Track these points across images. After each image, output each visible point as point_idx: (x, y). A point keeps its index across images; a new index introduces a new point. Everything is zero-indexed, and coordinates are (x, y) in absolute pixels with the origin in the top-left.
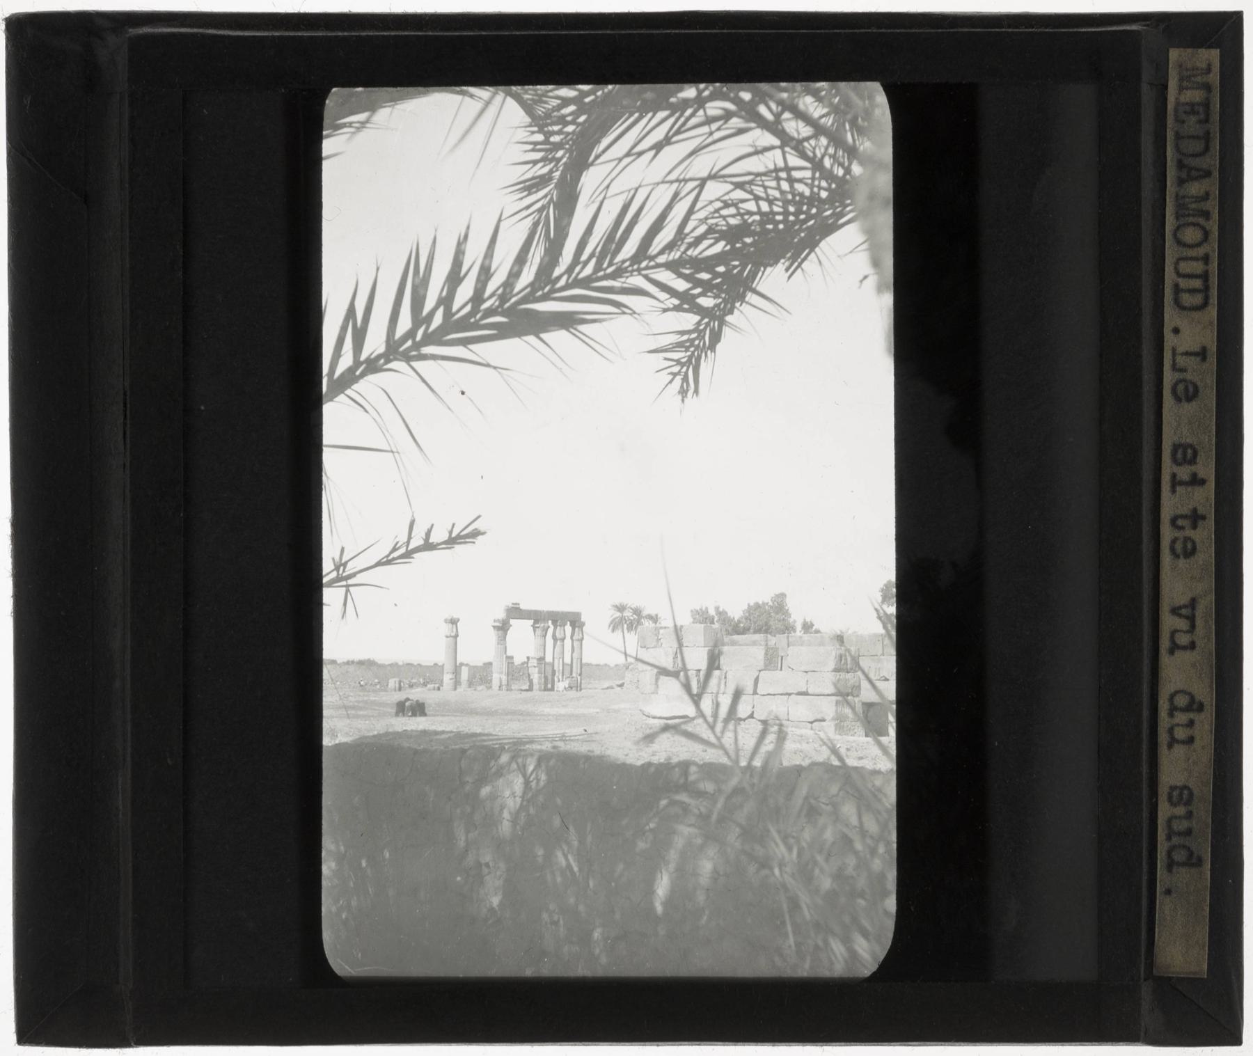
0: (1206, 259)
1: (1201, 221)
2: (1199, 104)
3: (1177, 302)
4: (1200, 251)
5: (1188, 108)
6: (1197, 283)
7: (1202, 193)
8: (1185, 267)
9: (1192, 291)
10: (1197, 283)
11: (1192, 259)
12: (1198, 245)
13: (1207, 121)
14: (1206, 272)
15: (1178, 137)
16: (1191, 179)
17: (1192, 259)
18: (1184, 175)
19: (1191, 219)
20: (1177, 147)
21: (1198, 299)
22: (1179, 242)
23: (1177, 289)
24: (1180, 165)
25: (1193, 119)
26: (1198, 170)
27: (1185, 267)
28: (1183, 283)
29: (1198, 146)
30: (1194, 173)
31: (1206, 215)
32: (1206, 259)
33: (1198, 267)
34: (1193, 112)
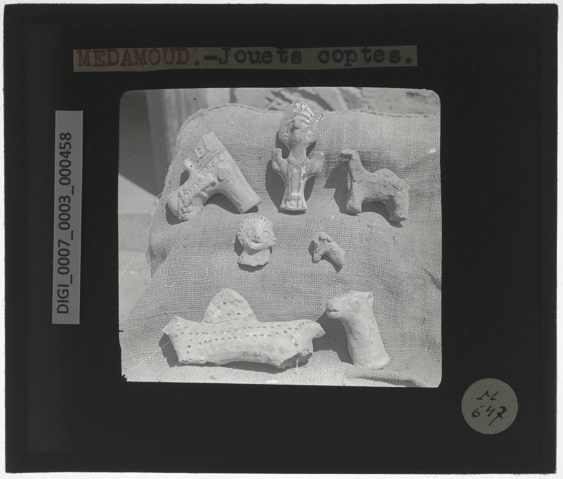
6: (176, 53)
8: (169, 59)
15: (110, 64)
26: (125, 56)
28: (176, 60)
29: (113, 55)
31: (143, 51)
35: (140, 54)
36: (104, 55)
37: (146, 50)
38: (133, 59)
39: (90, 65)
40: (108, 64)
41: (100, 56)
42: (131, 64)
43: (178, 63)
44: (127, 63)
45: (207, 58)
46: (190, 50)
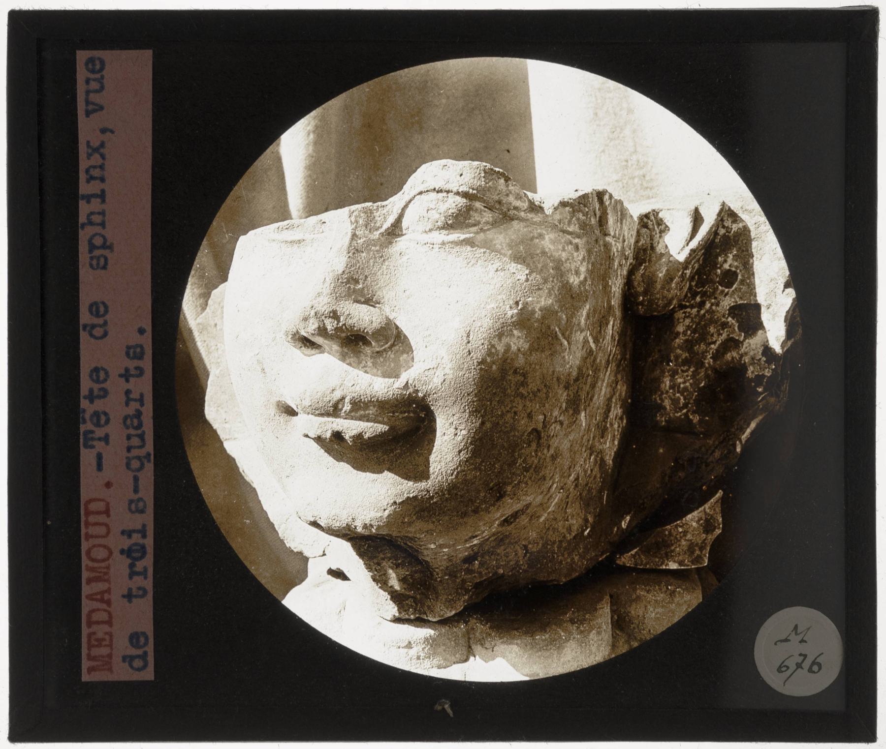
0: (88, 537)
1: (91, 564)
2: (94, 646)
3: (108, 504)
4: (92, 542)
5: (104, 643)
6: (92, 519)
7: (93, 584)
8: (102, 530)
9: (98, 513)
11: (97, 537)
12: (94, 546)
13: (90, 636)
14: (87, 527)
15: (109, 623)
17: (97, 537)
19: (96, 565)
20: (110, 614)
21: (93, 507)
22: (105, 547)
23: (107, 512)
24: (108, 602)
25: (100, 635)
26: (96, 600)
28: (102, 518)
30: (99, 597)
31: (90, 569)
33: (92, 530)
34: (100, 641)
36: (94, 633)
37: (87, 565)
39: (110, 656)
42: (108, 591)
43: (108, 516)
44: (106, 597)
45: (100, 467)
46: (85, 494)
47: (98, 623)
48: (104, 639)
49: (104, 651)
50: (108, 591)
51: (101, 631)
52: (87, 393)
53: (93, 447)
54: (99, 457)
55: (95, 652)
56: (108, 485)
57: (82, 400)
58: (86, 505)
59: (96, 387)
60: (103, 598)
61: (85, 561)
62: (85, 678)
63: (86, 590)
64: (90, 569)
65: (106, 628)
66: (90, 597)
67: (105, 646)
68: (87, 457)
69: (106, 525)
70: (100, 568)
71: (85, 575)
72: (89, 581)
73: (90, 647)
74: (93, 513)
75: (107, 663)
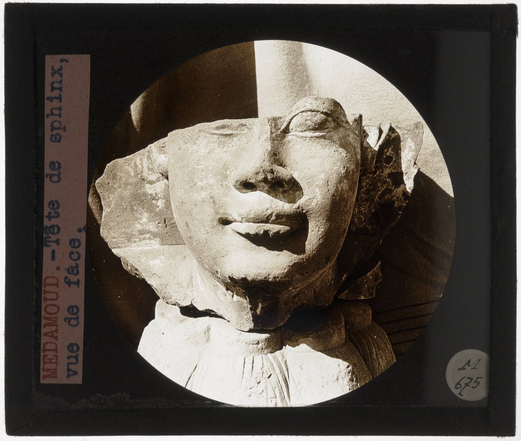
0: (46, 299)
6: (48, 288)
7: (47, 327)
10: (48, 288)
14: (44, 294)
15: (56, 350)
16: (52, 332)
18: (55, 334)
21: (49, 281)
23: (57, 285)
24: (56, 338)
27: (54, 296)
30: (50, 334)
31: (45, 318)
32: (46, 299)
33: (48, 296)
34: (50, 359)
35: (48, 322)
36: (47, 355)
38: (54, 328)
39: (55, 369)
40: (57, 352)
41: (48, 359)
42: (56, 331)
44: (55, 334)
45: (53, 258)
47: (49, 350)
48: (53, 359)
49: (53, 366)
50: (56, 331)
51: (50, 355)
52: (47, 214)
53: (49, 246)
54: (53, 252)
55: (48, 366)
56: (58, 269)
57: (45, 219)
58: (45, 280)
59: (53, 212)
60: (53, 335)
61: (43, 313)
62: (42, 381)
63: (43, 330)
64: (45, 318)
65: (55, 353)
66: (46, 334)
67: (53, 363)
68: (47, 252)
69: (57, 294)
70: (52, 318)
71: (43, 322)
72: (45, 325)
73: (45, 363)
74: (50, 285)
75: (54, 373)
